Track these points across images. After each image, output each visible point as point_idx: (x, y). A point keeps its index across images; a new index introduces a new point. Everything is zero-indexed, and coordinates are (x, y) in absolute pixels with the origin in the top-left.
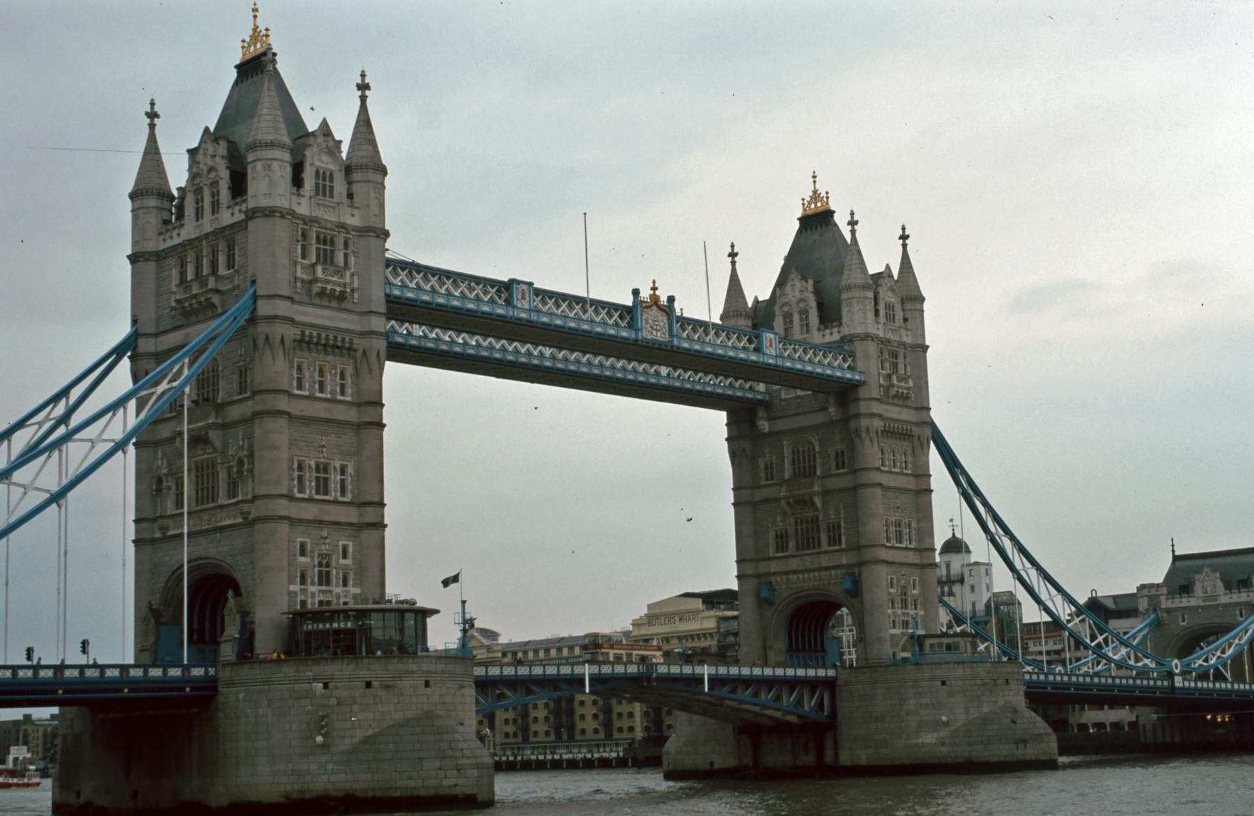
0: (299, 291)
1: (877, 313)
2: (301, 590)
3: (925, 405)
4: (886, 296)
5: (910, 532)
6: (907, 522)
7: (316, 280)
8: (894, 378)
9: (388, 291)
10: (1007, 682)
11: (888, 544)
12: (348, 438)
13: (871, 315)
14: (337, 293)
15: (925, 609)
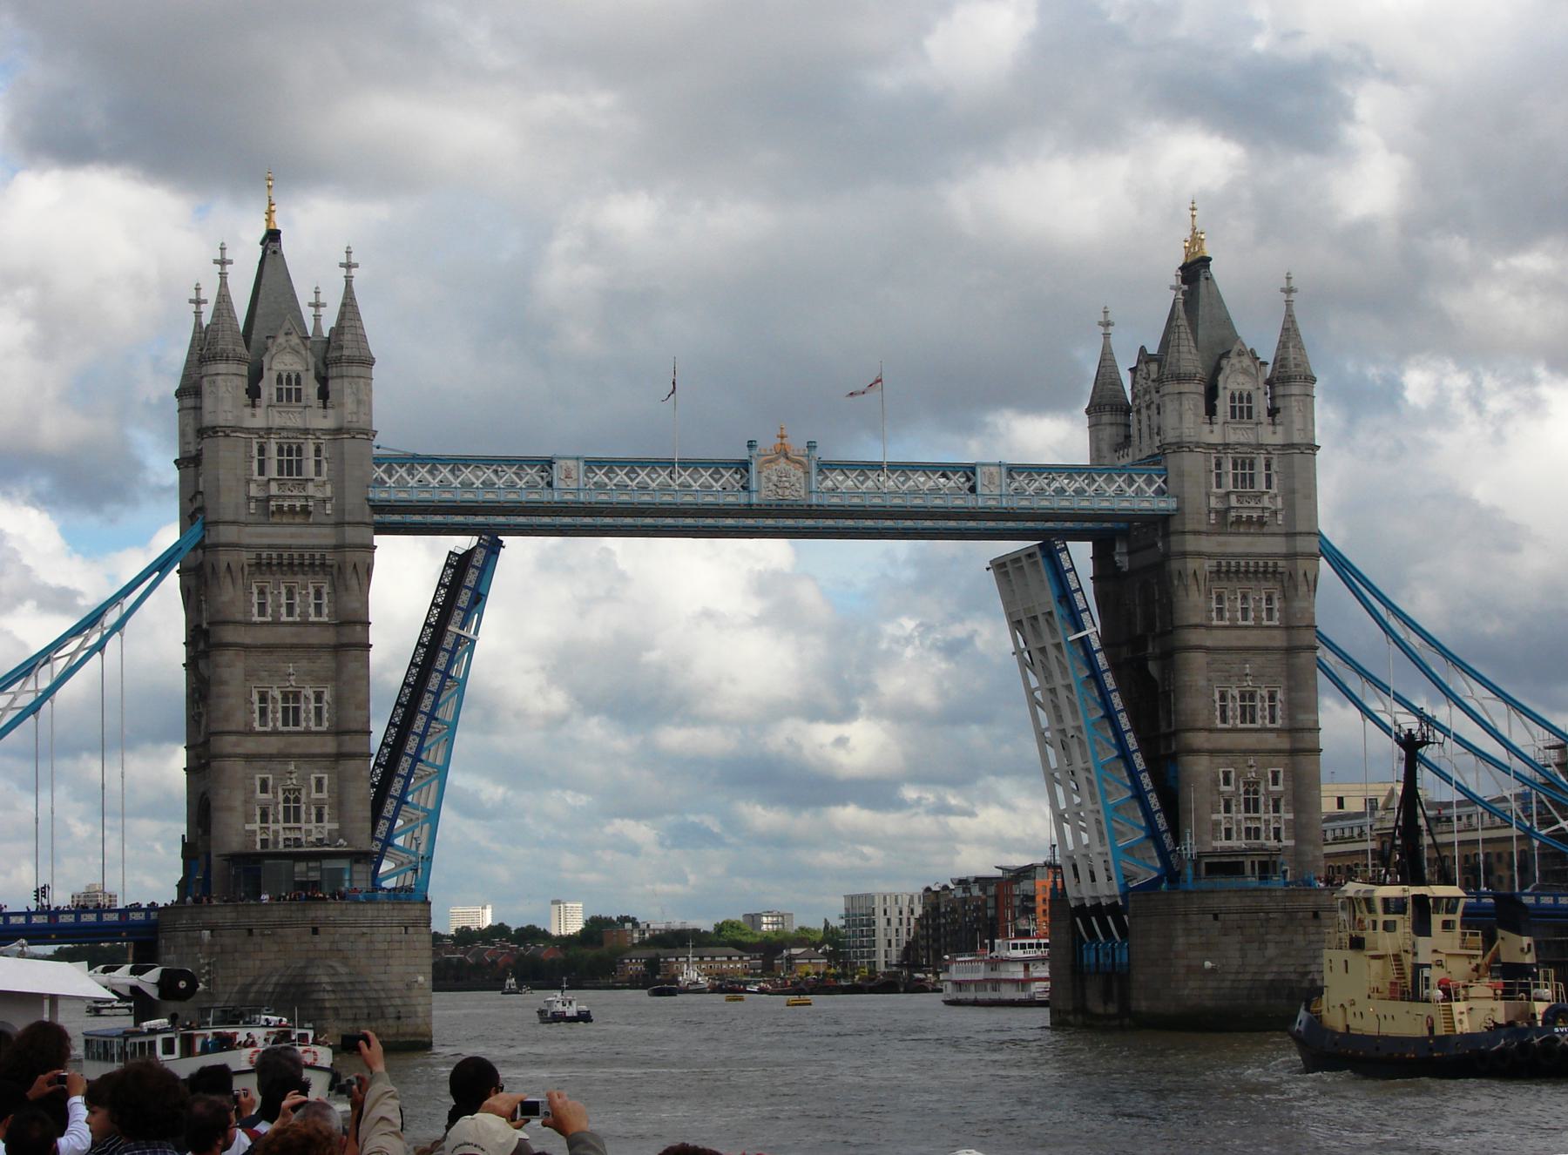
0: (252, 511)
1: (1211, 411)
2: (261, 828)
3: (1299, 528)
4: (1233, 382)
5: (1272, 708)
6: (1265, 693)
7: (269, 499)
8: (1233, 498)
9: (371, 496)
10: (1316, 915)
11: (1220, 725)
12: (325, 662)
13: (1189, 418)
14: (298, 509)
15: (1296, 812)
